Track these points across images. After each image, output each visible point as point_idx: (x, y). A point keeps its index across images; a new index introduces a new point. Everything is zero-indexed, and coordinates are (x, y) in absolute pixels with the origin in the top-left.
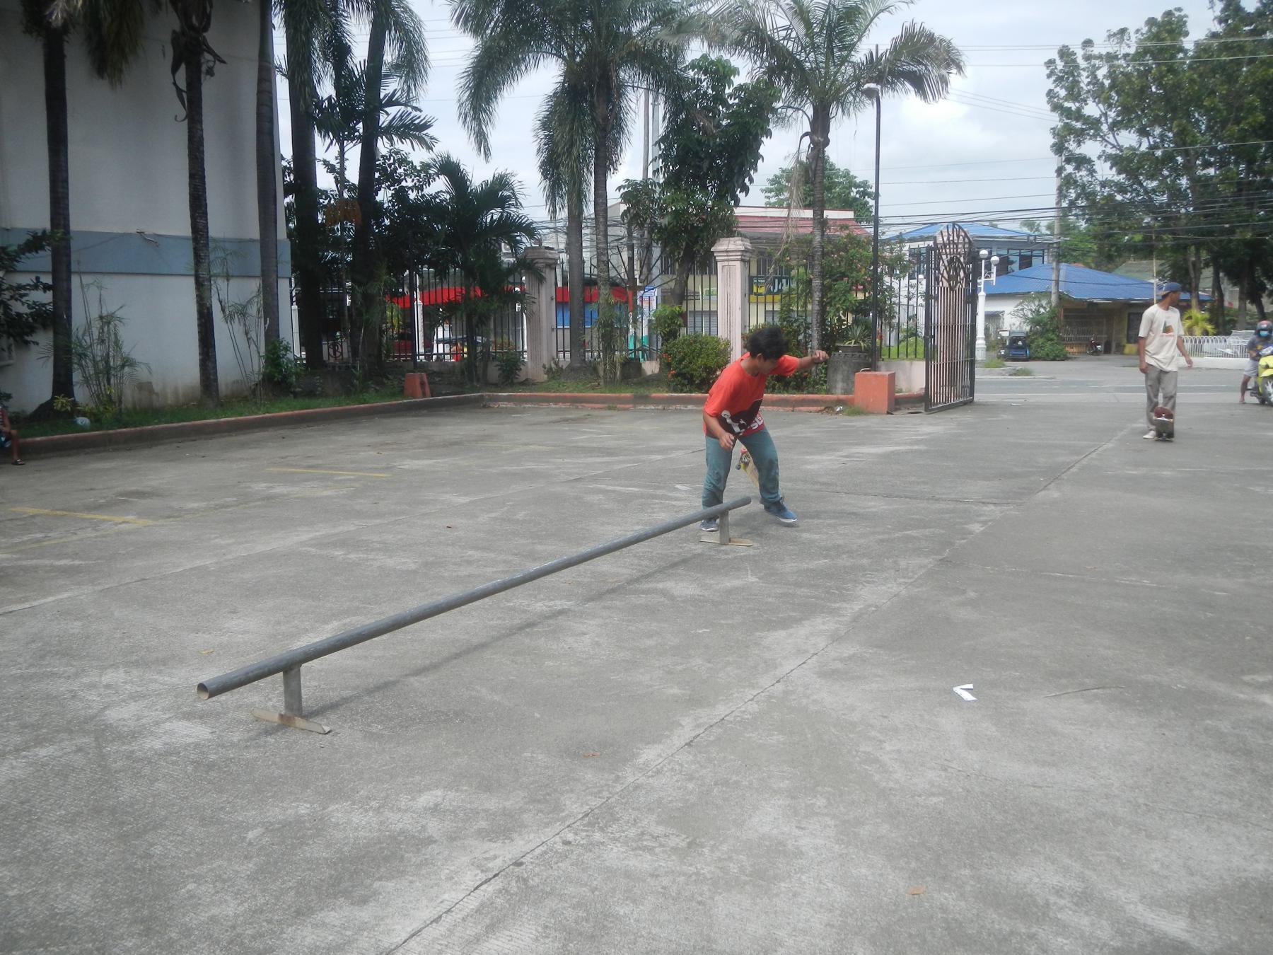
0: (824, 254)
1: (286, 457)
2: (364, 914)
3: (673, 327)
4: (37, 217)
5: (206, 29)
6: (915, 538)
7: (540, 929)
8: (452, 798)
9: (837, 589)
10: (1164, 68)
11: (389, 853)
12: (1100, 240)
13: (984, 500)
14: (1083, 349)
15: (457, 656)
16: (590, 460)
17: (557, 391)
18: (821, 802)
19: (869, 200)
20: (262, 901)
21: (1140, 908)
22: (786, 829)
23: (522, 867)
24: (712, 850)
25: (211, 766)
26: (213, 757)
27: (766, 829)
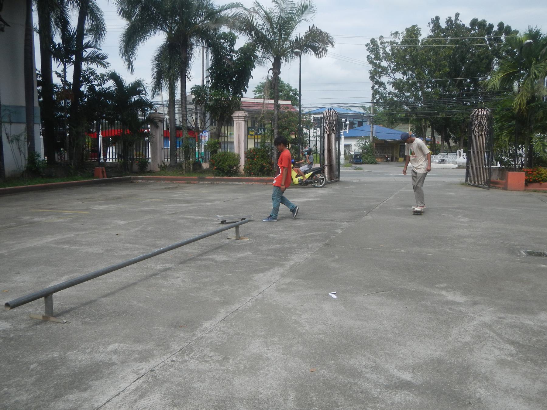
0: (279, 119)
1: (39, 205)
2: (86, 395)
3: (215, 148)
6: (315, 235)
7: (162, 395)
8: (123, 346)
9: (284, 256)
10: (413, 49)
11: (96, 370)
12: (389, 116)
13: (342, 220)
14: (383, 160)
15: (122, 289)
16: (179, 205)
17: (165, 175)
18: (277, 339)
19: (297, 97)
20: (39, 393)
21: (395, 370)
22: (263, 350)
23: (155, 372)
24: (233, 359)
25: (11, 339)
26: (12, 335)
27: (255, 351)
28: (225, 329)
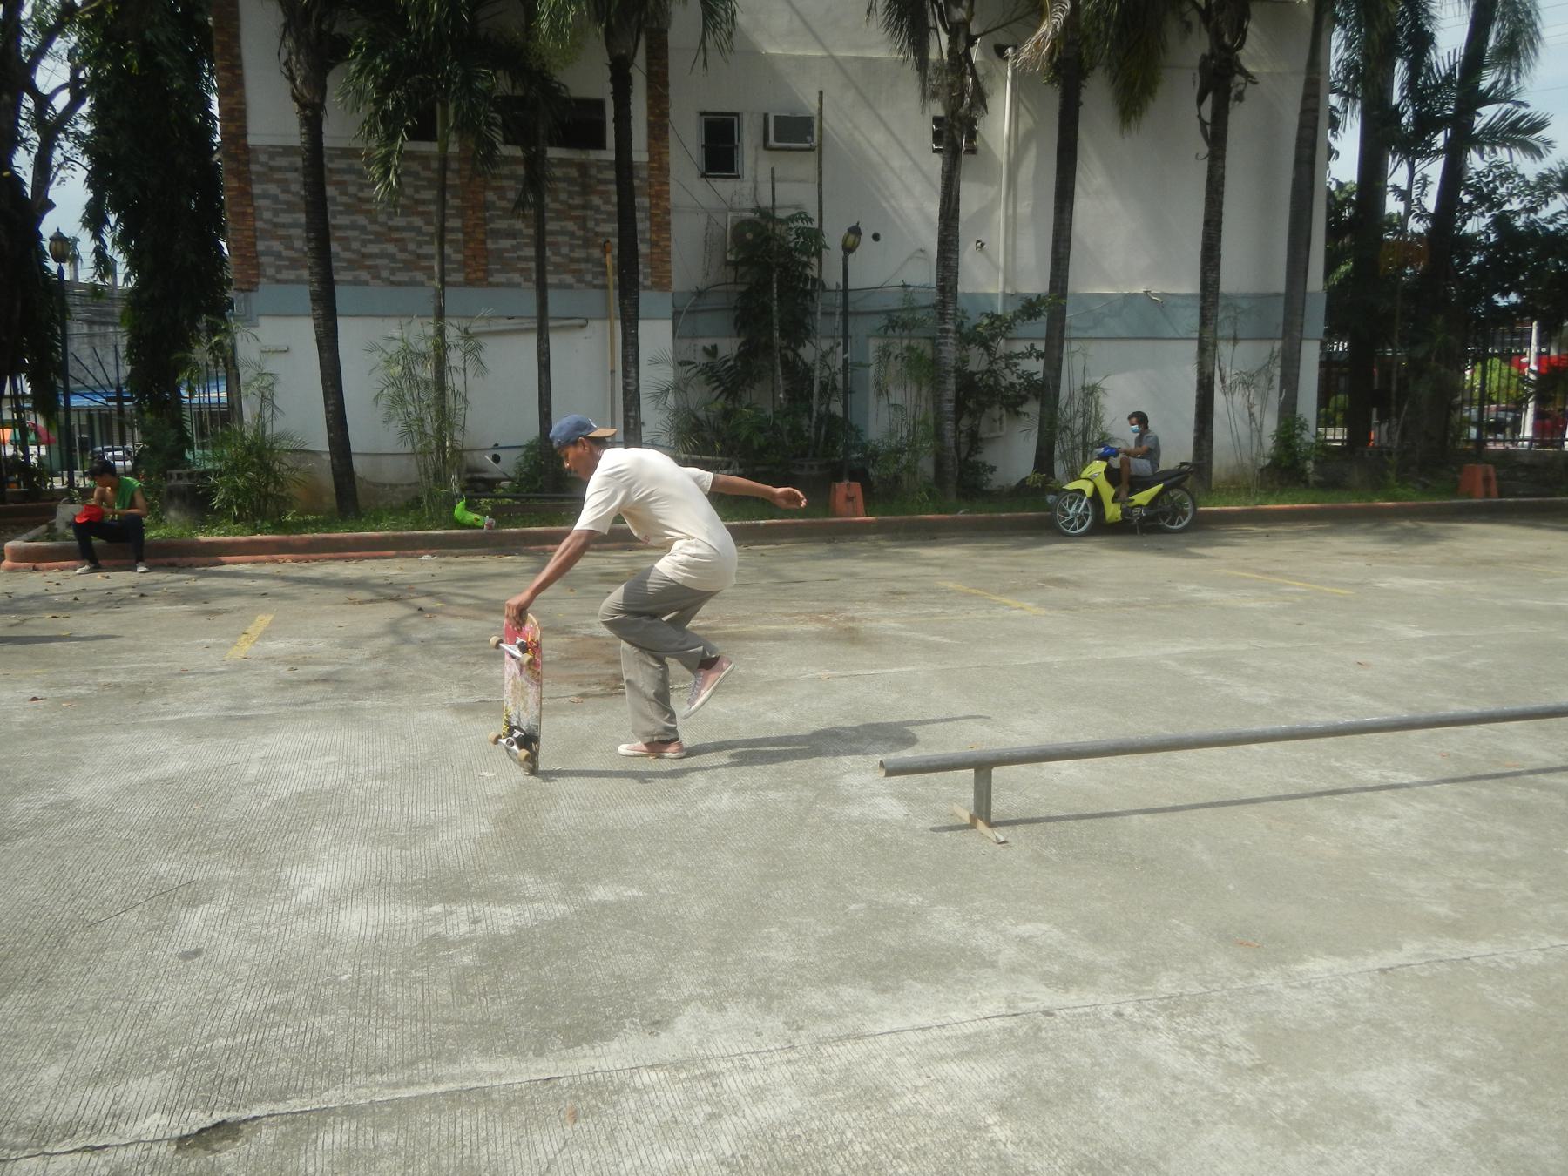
2: (873, 1000)
4: (1036, 283)
5: (1241, 46)
7: (1006, 1074)
24: (1272, 1083)
26: (887, 835)
28: (1359, 995)
